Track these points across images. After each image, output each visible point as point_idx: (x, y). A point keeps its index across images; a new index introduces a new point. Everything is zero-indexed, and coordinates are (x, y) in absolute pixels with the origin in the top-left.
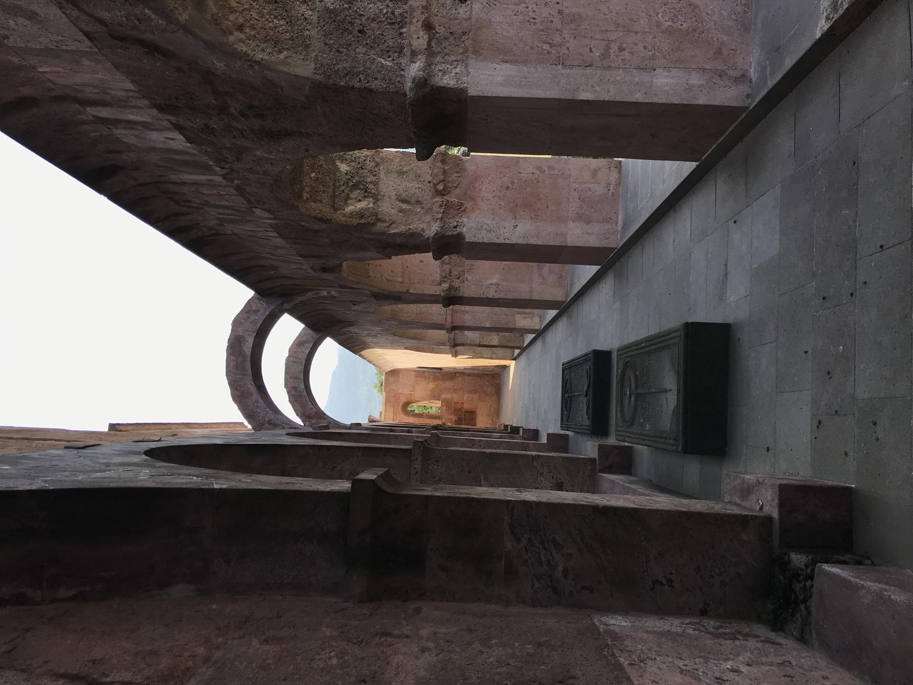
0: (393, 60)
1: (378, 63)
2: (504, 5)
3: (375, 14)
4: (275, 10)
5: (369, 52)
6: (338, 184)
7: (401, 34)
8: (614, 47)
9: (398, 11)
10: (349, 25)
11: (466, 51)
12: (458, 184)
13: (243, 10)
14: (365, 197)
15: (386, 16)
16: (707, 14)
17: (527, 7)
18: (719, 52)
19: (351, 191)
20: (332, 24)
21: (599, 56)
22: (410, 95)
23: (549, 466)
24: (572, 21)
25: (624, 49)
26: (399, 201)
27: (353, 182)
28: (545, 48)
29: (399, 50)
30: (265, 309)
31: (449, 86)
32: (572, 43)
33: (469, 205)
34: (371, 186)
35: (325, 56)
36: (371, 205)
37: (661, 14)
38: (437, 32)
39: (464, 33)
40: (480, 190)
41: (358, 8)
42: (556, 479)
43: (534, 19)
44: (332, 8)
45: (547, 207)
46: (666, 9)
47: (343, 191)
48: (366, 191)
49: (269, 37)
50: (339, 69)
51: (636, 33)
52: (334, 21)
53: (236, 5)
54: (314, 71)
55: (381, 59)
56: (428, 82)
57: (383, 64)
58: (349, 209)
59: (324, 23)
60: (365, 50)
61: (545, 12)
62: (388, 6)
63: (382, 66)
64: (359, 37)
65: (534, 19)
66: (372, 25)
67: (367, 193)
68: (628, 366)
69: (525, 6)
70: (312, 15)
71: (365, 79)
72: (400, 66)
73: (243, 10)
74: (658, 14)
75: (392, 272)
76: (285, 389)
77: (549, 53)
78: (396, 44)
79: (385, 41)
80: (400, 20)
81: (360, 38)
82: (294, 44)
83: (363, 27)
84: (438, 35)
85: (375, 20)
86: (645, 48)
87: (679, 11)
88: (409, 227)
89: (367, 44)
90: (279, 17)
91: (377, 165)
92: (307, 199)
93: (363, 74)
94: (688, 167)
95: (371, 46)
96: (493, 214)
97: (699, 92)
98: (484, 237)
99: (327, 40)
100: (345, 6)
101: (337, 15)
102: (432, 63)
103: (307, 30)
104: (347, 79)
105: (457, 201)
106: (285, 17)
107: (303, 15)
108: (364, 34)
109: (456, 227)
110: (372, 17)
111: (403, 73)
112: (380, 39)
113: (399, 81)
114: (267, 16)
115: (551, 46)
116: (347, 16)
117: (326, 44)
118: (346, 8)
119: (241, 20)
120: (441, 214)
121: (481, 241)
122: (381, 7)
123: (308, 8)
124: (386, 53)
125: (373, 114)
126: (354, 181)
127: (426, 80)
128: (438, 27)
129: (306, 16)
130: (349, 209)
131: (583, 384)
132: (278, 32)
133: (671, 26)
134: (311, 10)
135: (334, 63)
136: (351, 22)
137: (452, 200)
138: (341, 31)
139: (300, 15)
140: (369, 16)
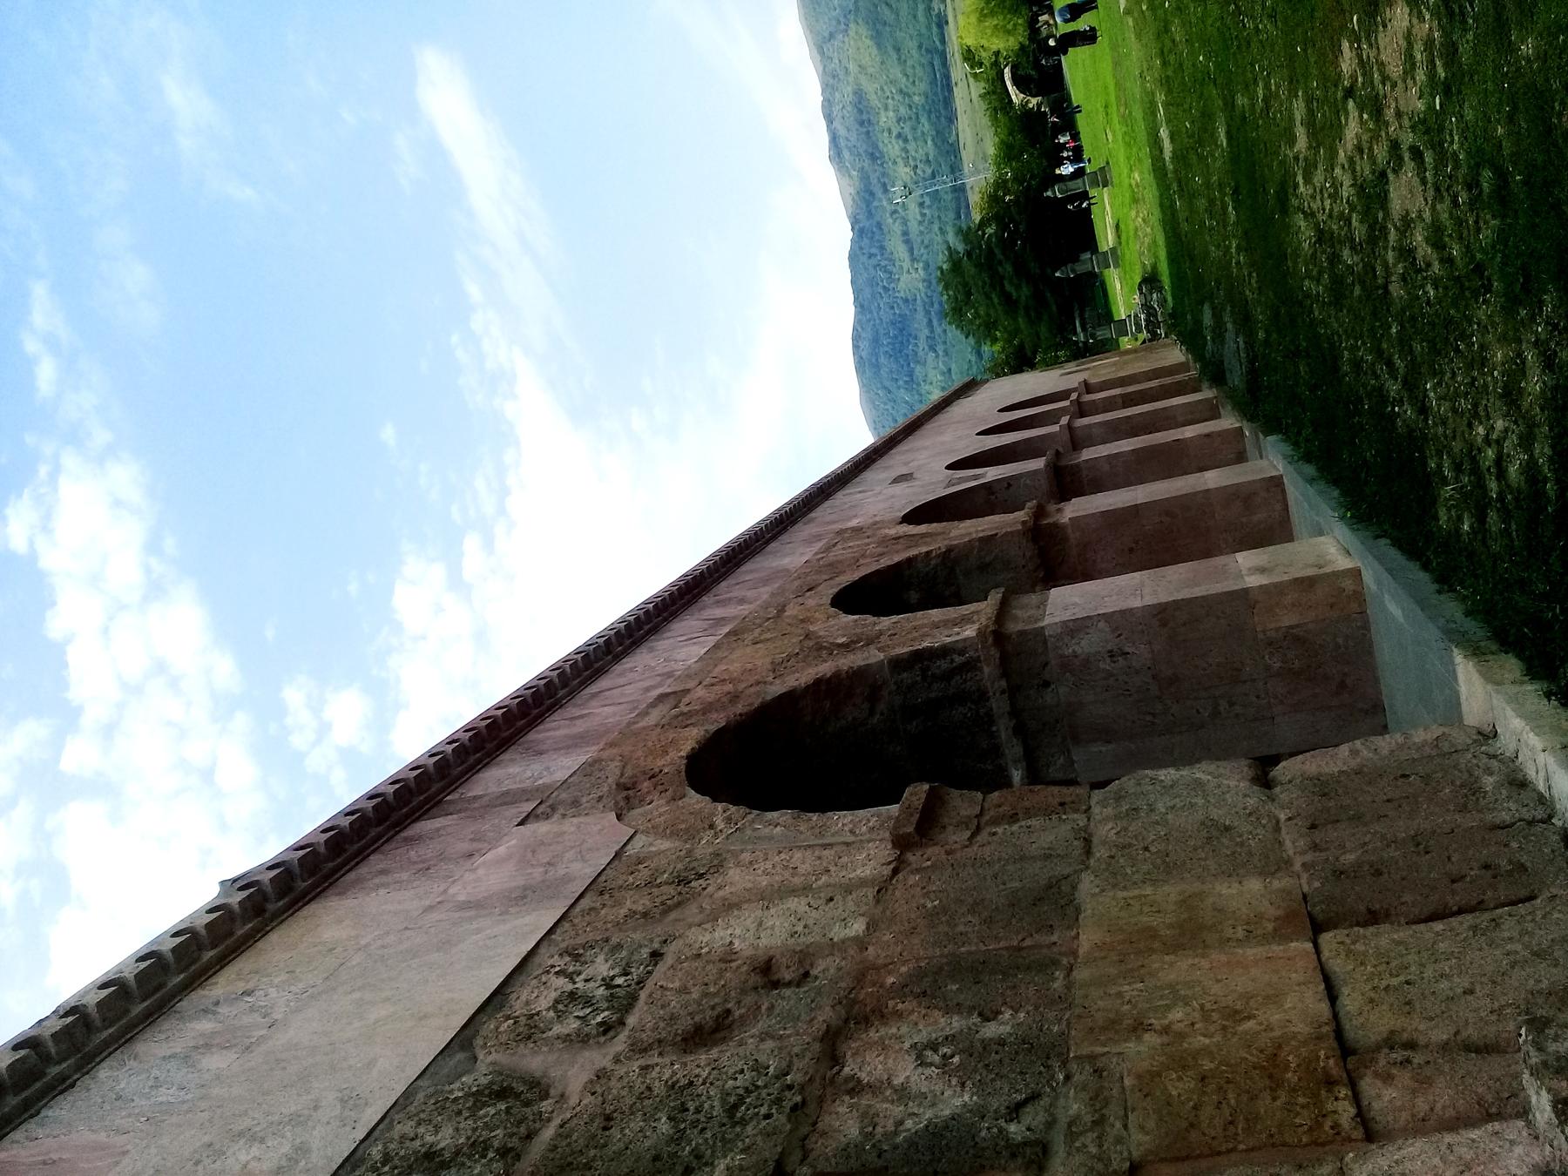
8: (1223, 705)
17: (1117, 680)
37: (1267, 657)
39: (1057, 721)
40: (1094, 561)
51: (1245, 682)
62: (970, 709)
74: (1264, 657)
77: (1153, 723)
86: (1258, 697)
115: (1154, 715)
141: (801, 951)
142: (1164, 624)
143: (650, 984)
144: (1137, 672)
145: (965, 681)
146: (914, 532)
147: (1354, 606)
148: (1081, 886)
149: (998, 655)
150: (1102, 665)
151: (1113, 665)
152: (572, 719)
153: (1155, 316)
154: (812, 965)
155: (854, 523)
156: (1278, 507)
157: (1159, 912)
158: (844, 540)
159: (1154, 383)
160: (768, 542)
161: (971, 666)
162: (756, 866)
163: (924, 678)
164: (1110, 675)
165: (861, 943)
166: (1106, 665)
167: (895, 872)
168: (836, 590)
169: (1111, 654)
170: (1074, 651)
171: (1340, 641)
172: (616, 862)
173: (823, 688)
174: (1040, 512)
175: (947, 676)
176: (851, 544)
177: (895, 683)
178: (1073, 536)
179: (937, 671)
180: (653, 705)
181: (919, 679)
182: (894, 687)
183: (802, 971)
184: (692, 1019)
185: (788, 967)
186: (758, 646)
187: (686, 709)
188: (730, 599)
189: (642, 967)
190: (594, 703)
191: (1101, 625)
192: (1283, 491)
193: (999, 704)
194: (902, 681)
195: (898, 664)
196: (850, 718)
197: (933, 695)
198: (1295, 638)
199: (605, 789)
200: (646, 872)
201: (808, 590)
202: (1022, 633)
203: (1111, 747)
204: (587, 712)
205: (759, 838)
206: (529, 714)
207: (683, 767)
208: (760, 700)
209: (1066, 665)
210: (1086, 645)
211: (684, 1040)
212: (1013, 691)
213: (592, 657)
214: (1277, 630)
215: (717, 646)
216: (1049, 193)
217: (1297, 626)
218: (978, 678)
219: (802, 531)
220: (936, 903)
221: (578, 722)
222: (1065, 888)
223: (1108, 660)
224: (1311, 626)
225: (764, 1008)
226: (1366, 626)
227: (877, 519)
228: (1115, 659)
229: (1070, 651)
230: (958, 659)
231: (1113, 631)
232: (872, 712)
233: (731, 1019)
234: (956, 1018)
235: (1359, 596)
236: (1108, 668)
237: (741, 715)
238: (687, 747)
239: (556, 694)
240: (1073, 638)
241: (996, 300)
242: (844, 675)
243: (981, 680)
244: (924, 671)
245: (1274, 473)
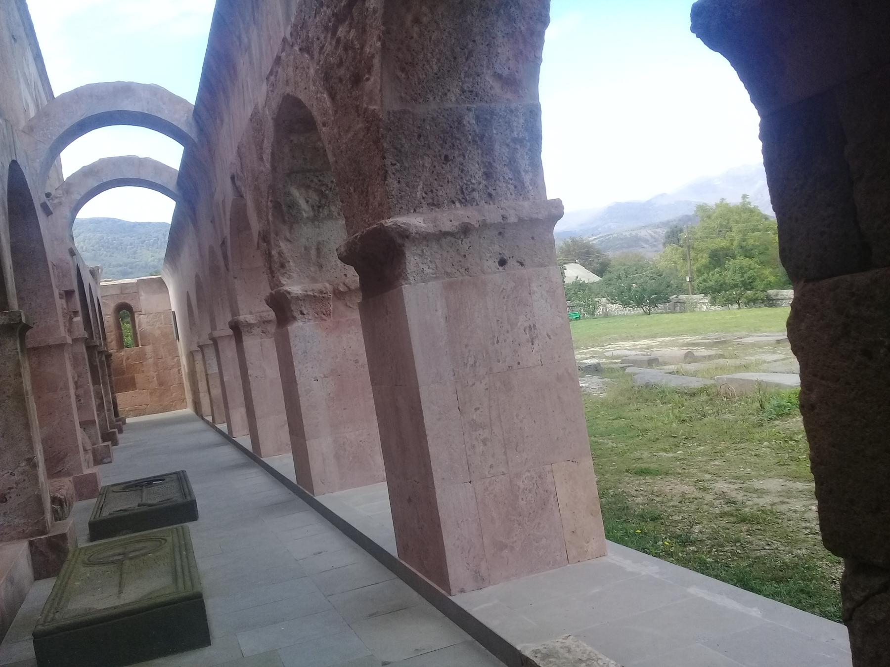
0: (423, 198)
1: (417, 182)
2: (505, 307)
3: (468, 171)
4: (447, 58)
5: (427, 171)
6: (318, 174)
7: (454, 202)
9: (476, 195)
10: (450, 144)
11: (448, 275)
12: (351, 307)
13: (436, 22)
14: (313, 207)
15: (469, 183)
16: (539, 523)
17: (508, 332)
18: (503, 546)
19: (316, 190)
20: (448, 125)
21: (473, 420)
22: (388, 223)
23: (24, 480)
25: (485, 445)
26: (318, 245)
27: (325, 191)
28: (469, 360)
29: (435, 203)
30: (182, 120)
31: (407, 263)
33: (329, 322)
34: (326, 212)
35: (411, 122)
36: (305, 215)
37: (529, 475)
38: (462, 241)
39: (467, 270)
40: (349, 332)
41: (470, 151)
42: (9, 493)
43: (498, 342)
44: (464, 122)
45: (344, 409)
46: (535, 479)
47: (312, 181)
48: (319, 207)
49: (415, 54)
50: (400, 139)
51: (505, 454)
52: (451, 127)
53: (440, 13)
54: (391, 112)
55: (422, 185)
56: (406, 239)
57: (417, 187)
58: (295, 193)
59: (446, 116)
60: (428, 165)
62: (480, 183)
63: (415, 187)
64: (440, 156)
65: (498, 342)
66: (457, 169)
67: (317, 208)
68: (161, 543)
69: (510, 330)
70: (451, 101)
71: (397, 171)
72: (419, 207)
73: (436, 22)
74: (529, 471)
75: (254, 256)
76: (98, 160)
77: (465, 364)
78: (441, 199)
79: (442, 186)
80: (468, 199)
81: (439, 158)
82: (415, 84)
83: (452, 160)
84: (460, 242)
85: (462, 172)
86: (491, 466)
87: (536, 493)
88: (290, 261)
89: (435, 167)
90: (440, 64)
92: (292, 141)
93: (401, 166)
94: (391, 548)
95: (433, 172)
96: (325, 351)
97: (457, 536)
98: (297, 347)
99: (428, 122)
100: (470, 137)
101: (458, 129)
102: (428, 241)
103: (435, 98)
104: (392, 150)
105: (331, 309)
106: (441, 70)
107: (449, 91)
108: (445, 163)
109: (302, 313)
110: (464, 168)
111: (412, 211)
112: (442, 180)
113: (402, 208)
114: (437, 50)
115: (474, 365)
116: (460, 140)
117: (424, 120)
118: (468, 138)
119: (425, 20)
120: (312, 294)
121: (291, 344)
122: (477, 176)
123: (458, 96)
124: (430, 190)
125: (367, 187)
126: (327, 192)
127: (408, 237)
128: (468, 241)
129: (448, 94)
130: (295, 193)
131: (153, 497)
132: (424, 65)
133: (519, 488)
134: (457, 100)
135: (405, 132)
136: (454, 145)
137: (331, 304)
138: (442, 135)
139: (448, 87)
140: (465, 164)
142: (559, 378)
144: (515, 351)
145: (507, 182)
150: (522, 318)
151: (522, 328)
166: (522, 322)
170: (534, 292)
171: (544, 541)
177: (517, 109)
179: (519, 155)
181: (515, 134)
194: (516, 116)
196: (500, 50)
197: (497, 146)
203: (442, 321)
218: (509, 195)
223: (526, 324)
228: (527, 331)
229: (535, 289)
230: (527, 178)
236: (519, 324)
240: (548, 292)
243: (506, 199)
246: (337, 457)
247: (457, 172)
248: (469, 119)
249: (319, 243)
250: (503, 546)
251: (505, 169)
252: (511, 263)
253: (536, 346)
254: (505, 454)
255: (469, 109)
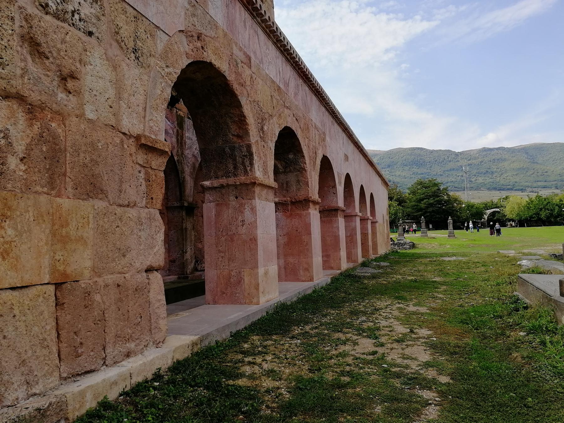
8: (222, 255)
11: (218, 201)
18: (224, 293)
24: (231, 238)
25: (222, 258)
32: (223, 239)
33: (288, 213)
51: (229, 262)
61: (234, 228)
63: (210, 172)
67: (285, 168)
86: (223, 266)
91: (299, 171)
115: (222, 232)
141: (81, 92)
142: (251, 240)
143: (72, 29)
144: (237, 228)
146: (317, 159)
147: (248, 301)
148: (101, 201)
149: (247, 182)
150: (240, 217)
152: (245, 22)
153: (401, 246)
154: (74, 95)
155: (328, 139)
156: (304, 279)
157: (78, 229)
158: (320, 135)
159: (370, 243)
160: (325, 107)
161: (246, 172)
162: (138, 81)
163: (244, 156)
164: (237, 219)
165: (80, 116)
166: (240, 218)
167: (124, 134)
168: (294, 129)
169: (243, 221)
171: (238, 295)
172: (154, 26)
173: (243, 118)
174: (315, 203)
175: (243, 164)
176: (317, 137)
177: (243, 145)
178: (304, 213)
180: (245, 53)
182: (241, 144)
183: (71, 91)
184: (44, 43)
185: (74, 86)
186: (270, 97)
187: (239, 66)
188: (298, 90)
189: (83, 27)
190: (252, 31)
191: (253, 219)
192: (308, 281)
193: (231, 181)
195: (249, 147)
197: (237, 158)
198: (240, 282)
199: (199, 28)
200: (144, 37)
201: (296, 119)
202: (254, 192)
204: (248, 27)
205: (156, 84)
206: (249, 5)
207: (205, 60)
208: (239, 94)
209: (242, 205)
210: (247, 213)
211: (31, 38)
212: (236, 186)
213: (275, 34)
214: (244, 276)
215: (273, 82)
216: (450, 218)
217: (244, 282)
219: (328, 119)
220: (100, 147)
221: (242, 24)
222: (100, 196)
223: (242, 220)
224: (243, 287)
225: (48, 73)
226: (241, 303)
227: (328, 148)
230: (248, 169)
231: (251, 223)
232: (233, 135)
233: (44, 59)
234: (24, 148)
235: (251, 303)
237: (232, 86)
238: (217, 63)
239: (259, 17)
241: (422, 196)
242: (247, 127)
244: (246, 156)
245: (314, 279)
246: (285, 268)
247: (224, 167)
248: (227, 149)
249: (287, 182)
250: (224, 293)
251: (241, 165)
252: (239, 198)
253: (244, 227)
254: (229, 262)
255: (226, 146)
